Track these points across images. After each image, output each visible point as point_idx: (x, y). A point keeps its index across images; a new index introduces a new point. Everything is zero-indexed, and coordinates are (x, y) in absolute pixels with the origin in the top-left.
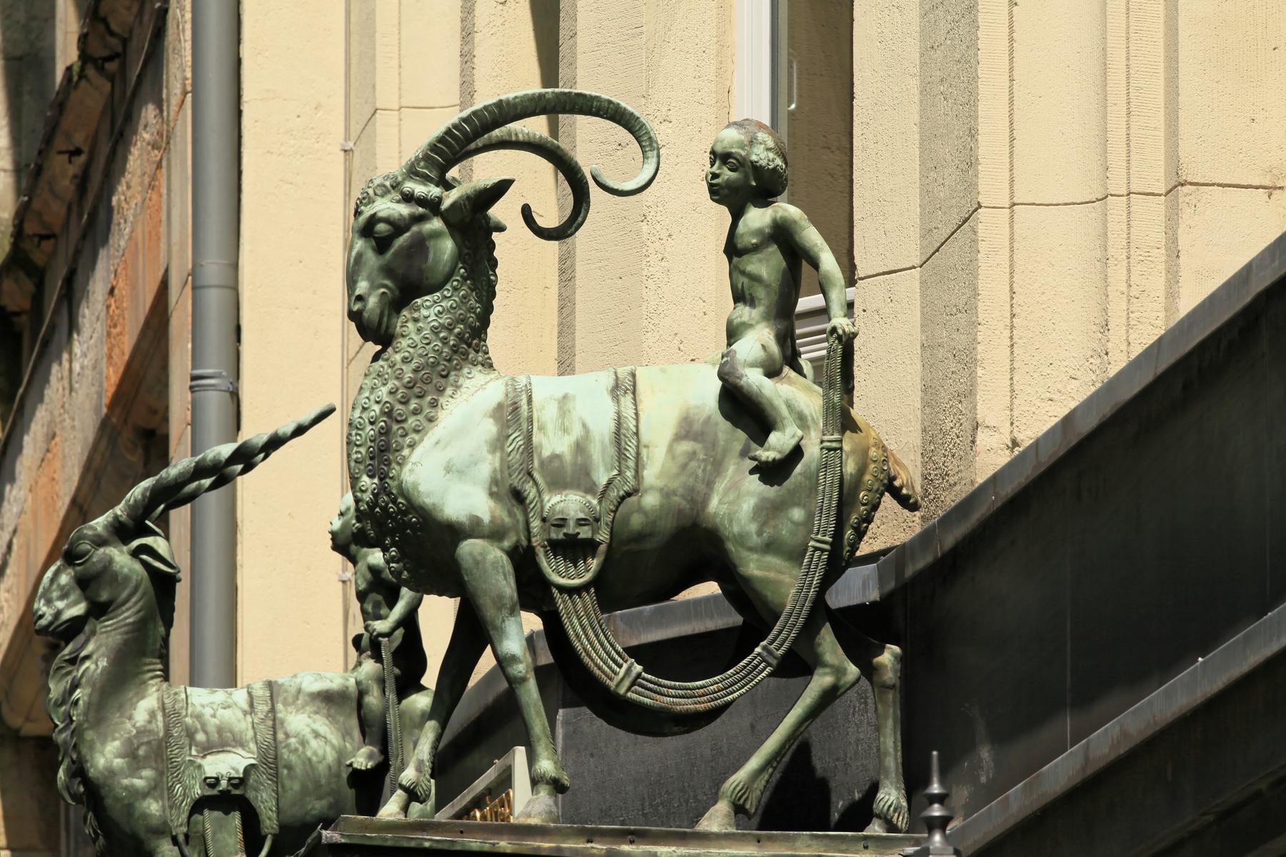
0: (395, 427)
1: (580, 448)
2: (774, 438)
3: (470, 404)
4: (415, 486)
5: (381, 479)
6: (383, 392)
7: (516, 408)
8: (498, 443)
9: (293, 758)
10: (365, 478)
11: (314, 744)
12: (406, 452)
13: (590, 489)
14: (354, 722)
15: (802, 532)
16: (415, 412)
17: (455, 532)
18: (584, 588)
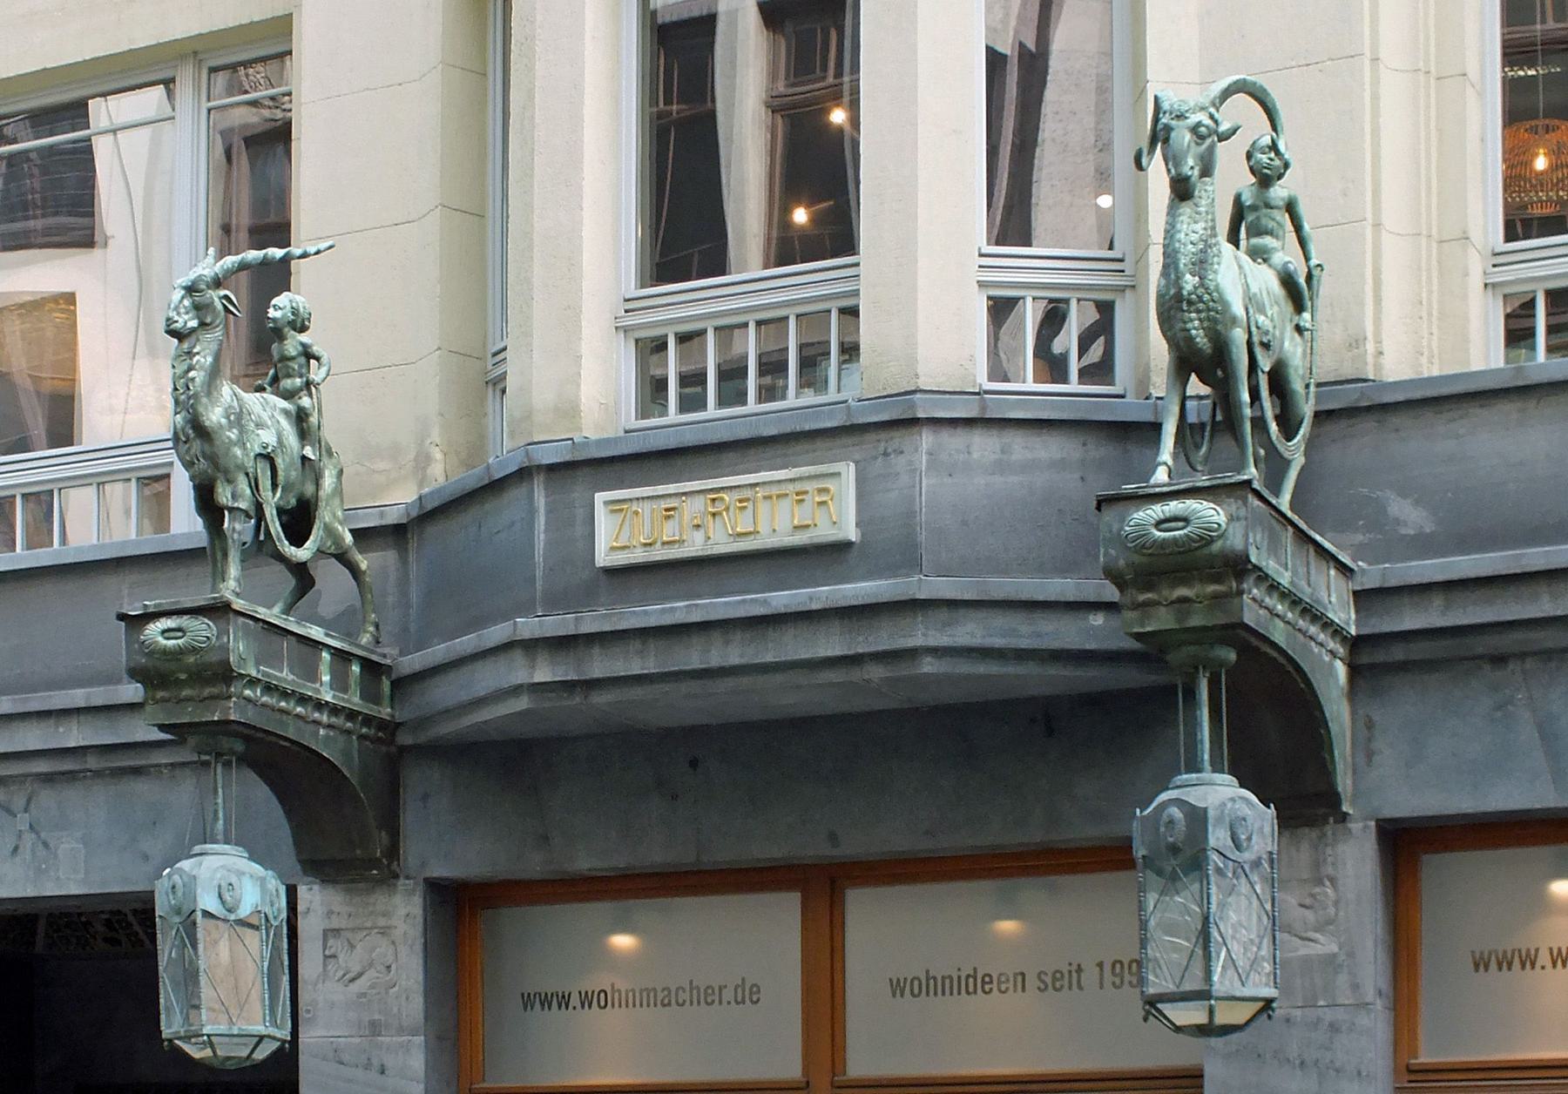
17: (1234, 321)
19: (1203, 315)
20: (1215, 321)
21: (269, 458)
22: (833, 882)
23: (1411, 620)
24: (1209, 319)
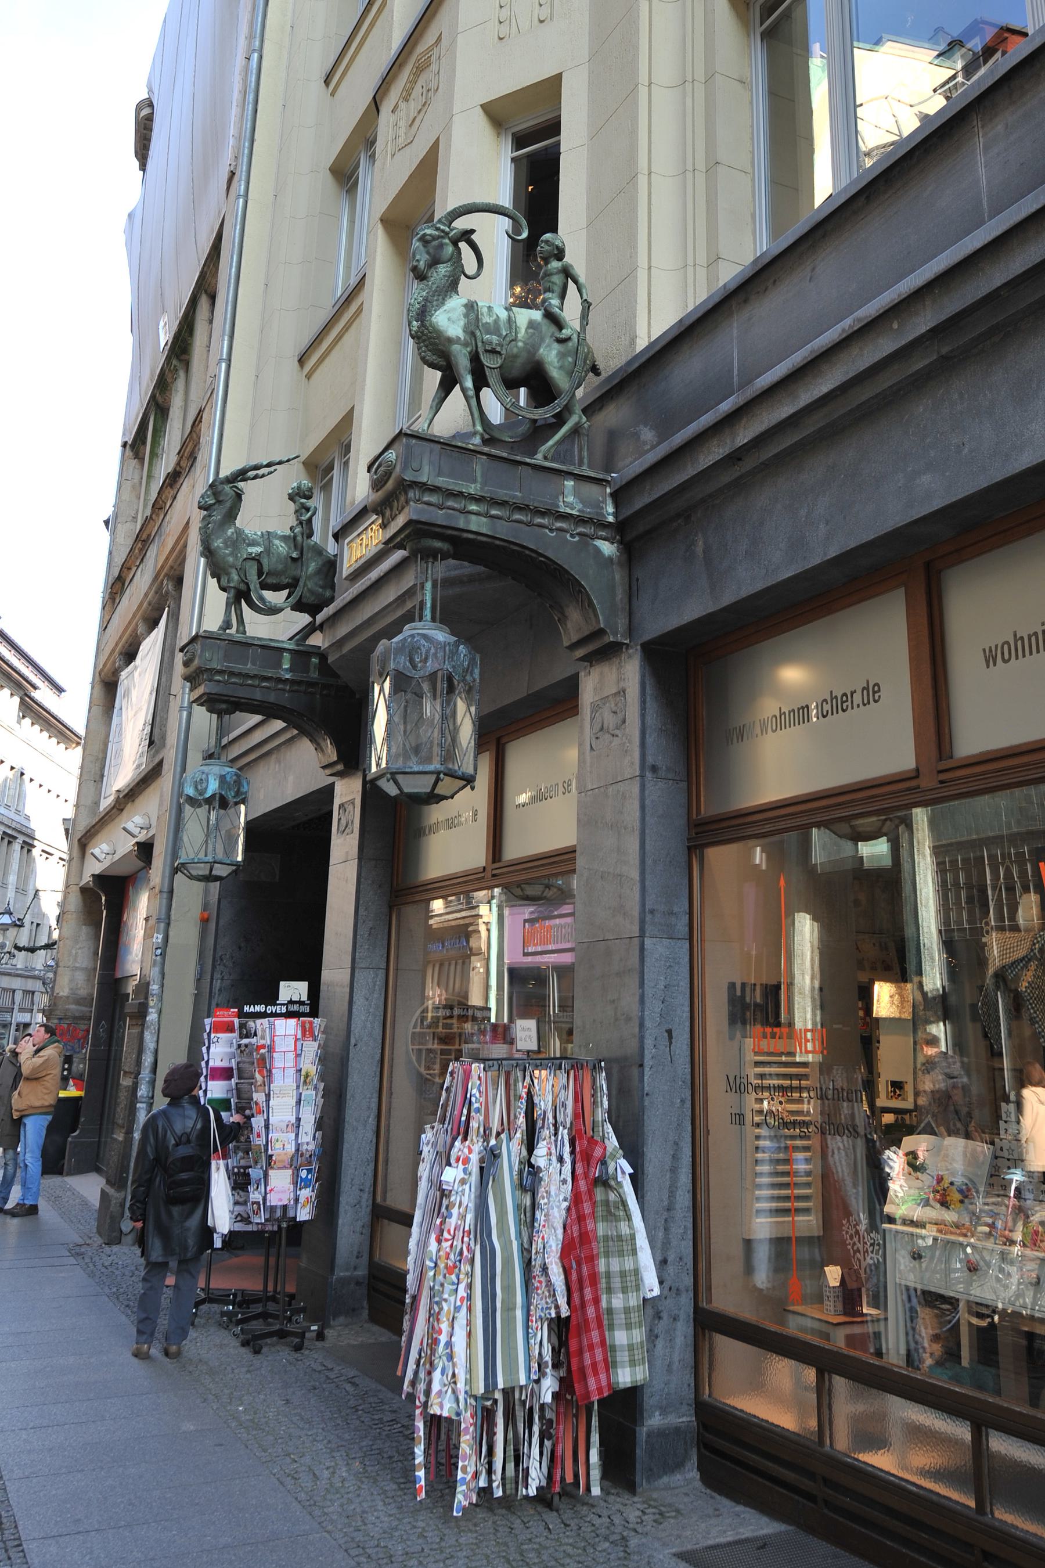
2: (564, 331)
3: (455, 304)
6: (424, 294)
7: (472, 306)
8: (466, 316)
13: (499, 335)
14: (292, 545)
17: (450, 340)
20: (435, 344)
21: (257, 559)
23: (640, 502)
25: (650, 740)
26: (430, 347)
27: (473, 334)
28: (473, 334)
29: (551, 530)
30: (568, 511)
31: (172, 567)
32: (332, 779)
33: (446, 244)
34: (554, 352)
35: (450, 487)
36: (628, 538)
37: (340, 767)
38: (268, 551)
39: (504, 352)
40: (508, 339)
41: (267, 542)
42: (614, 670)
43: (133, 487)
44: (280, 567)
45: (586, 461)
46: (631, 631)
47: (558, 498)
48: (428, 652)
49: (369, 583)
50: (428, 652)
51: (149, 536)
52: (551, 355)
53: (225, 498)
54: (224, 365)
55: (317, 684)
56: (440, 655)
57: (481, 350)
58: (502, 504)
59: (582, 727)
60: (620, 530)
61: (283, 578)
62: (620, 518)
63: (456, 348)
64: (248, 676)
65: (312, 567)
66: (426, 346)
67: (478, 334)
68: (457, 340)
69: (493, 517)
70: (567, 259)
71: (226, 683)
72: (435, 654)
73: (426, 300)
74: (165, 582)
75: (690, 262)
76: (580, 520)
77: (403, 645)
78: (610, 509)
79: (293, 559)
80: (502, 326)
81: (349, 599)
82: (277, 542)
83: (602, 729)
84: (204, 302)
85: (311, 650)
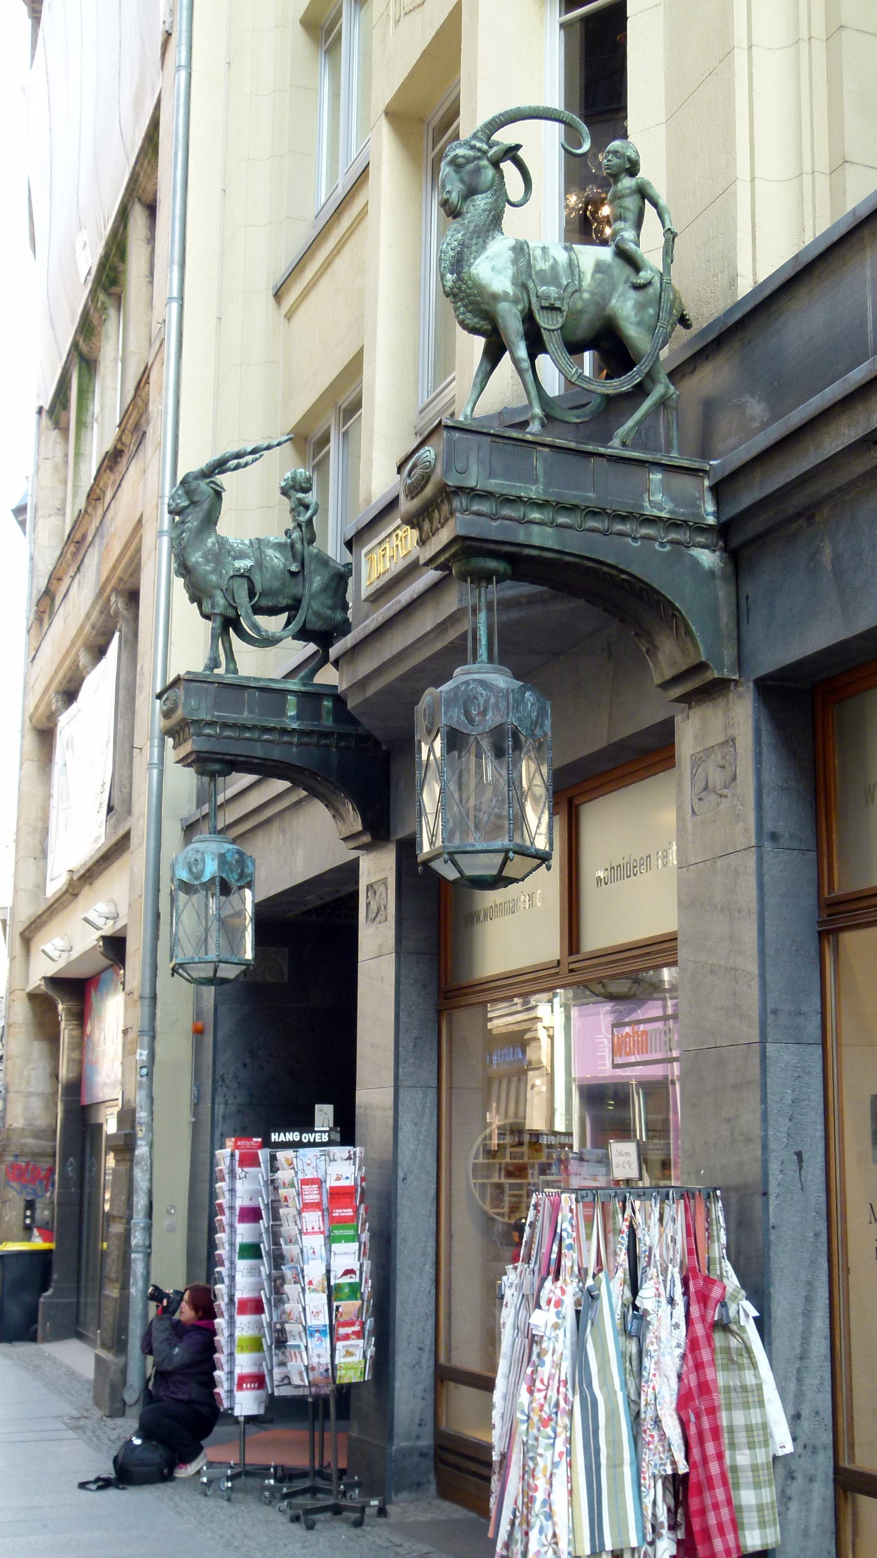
0: (465, 250)
1: (554, 267)
2: (642, 274)
3: (499, 248)
4: (478, 275)
5: (458, 274)
6: (459, 236)
7: (522, 249)
8: (515, 262)
9: (268, 565)
10: (449, 276)
11: (275, 560)
12: (472, 261)
13: (559, 286)
14: (290, 555)
15: (654, 320)
16: (476, 244)
17: (495, 297)
18: (557, 330)
19: (466, 301)
20: (477, 303)
21: (246, 576)
22: (570, 801)
23: (749, 496)
24: (472, 303)
25: (767, 801)
26: (470, 307)
27: (524, 287)
28: (524, 287)
29: (635, 539)
30: (656, 513)
31: (121, 579)
32: (354, 854)
33: (485, 167)
34: (630, 304)
35: (505, 492)
36: (735, 542)
37: (366, 839)
38: (260, 564)
39: (565, 308)
40: (570, 290)
41: (257, 553)
42: (720, 713)
43: (56, 468)
44: (276, 584)
45: (675, 442)
46: (740, 663)
47: (641, 496)
48: (487, 702)
49: (398, 608)
50: (487, 702)
51: (84, 536)
52: (626, 308)
53: (199, 499)
54: (175, 306)
55: (332, 733)
56: (502, 705)
57: (535, 308)
58: (572, 509)
59: (679, 785)
60: (724, 531)
61: (280, 598)
62: (724, 519)
63: (503, 307)
64: (245, 728)
65: (317, 582)
66: (465, 306)
67: (531, 285)
68: (505, 297)
69: (560, 526)
70: (644, 174)
71: (218, 737)
72: (496, 704)
73: (462, 244)
74: (113, 599)
75: (807, 168)
76: (673, 524)
77: (456, 694)
78: (710, 507)
79: (292, 574)
80: (561, 272)
81: (372, 627)
82: (270, 552)
83: (706, 788)
84: (138, 215)
85: (322, 691)
